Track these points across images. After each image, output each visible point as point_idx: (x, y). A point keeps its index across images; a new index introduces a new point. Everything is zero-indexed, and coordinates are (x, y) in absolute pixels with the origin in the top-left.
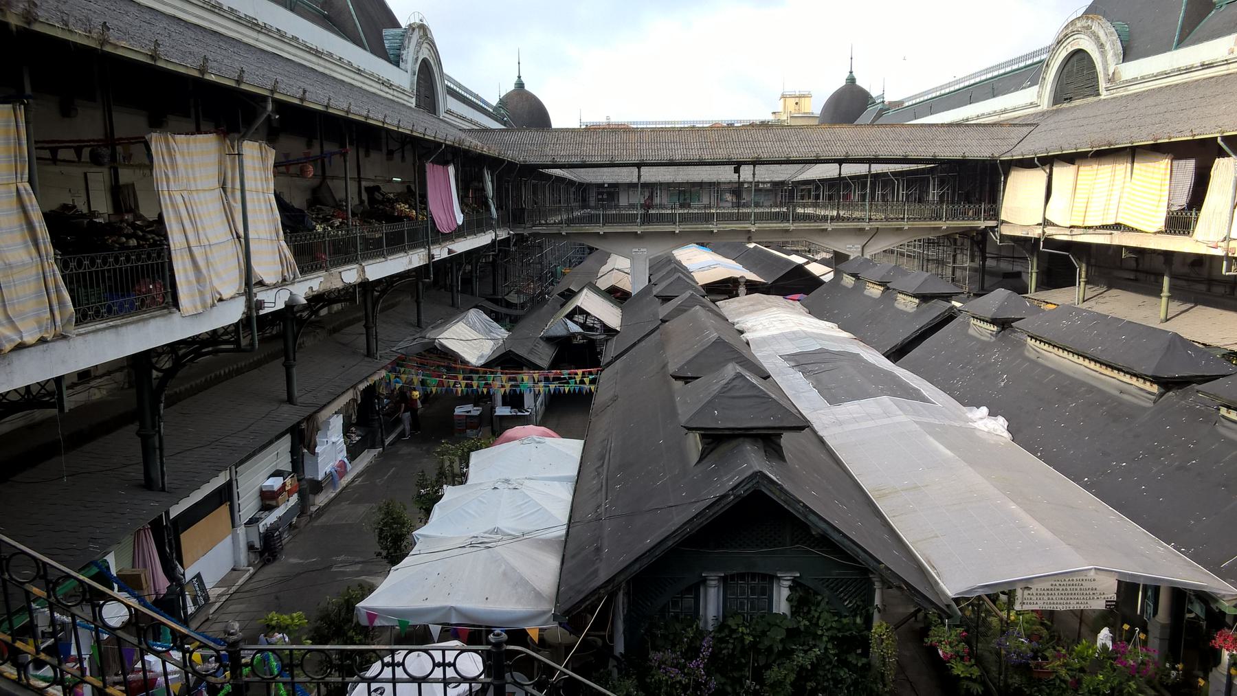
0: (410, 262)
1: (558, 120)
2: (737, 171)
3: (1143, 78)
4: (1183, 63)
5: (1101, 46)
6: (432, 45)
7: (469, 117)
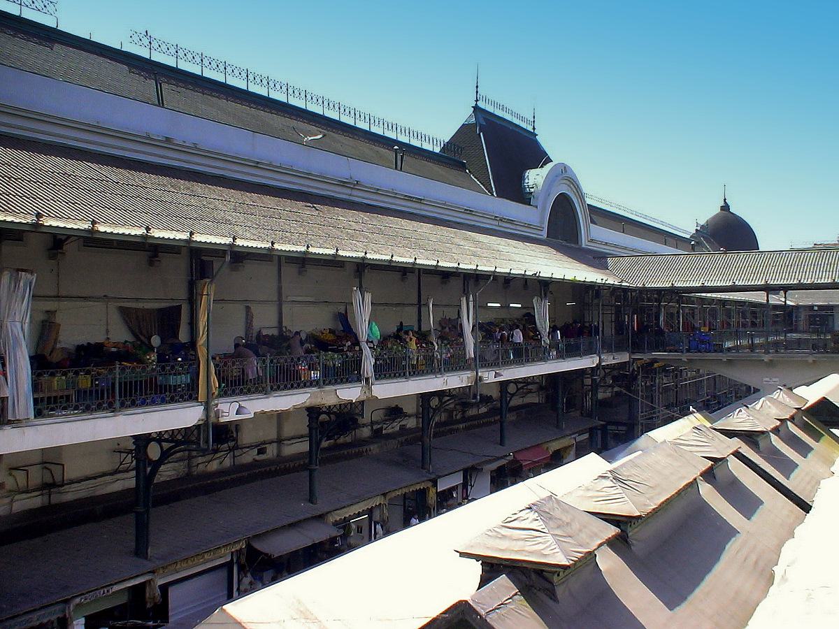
6: (573, 182)
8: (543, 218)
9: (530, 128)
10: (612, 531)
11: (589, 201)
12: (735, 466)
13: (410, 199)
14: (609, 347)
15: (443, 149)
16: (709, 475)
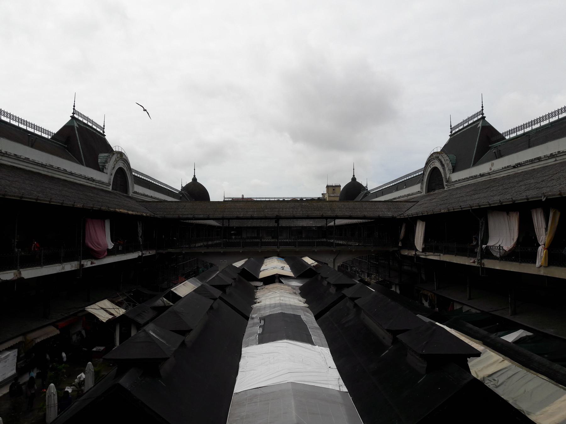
0: (63, 268)
2: (276, 222)
3: (459, 180)
4: (473, 174)
6: (126, 162)
7: (149, 194)
8: (110, 179)
9: (101, 132)
10: (180, 338)
11: (133, 173)
13: (38, 164)
14: (146, 248)
15: (52, 138)
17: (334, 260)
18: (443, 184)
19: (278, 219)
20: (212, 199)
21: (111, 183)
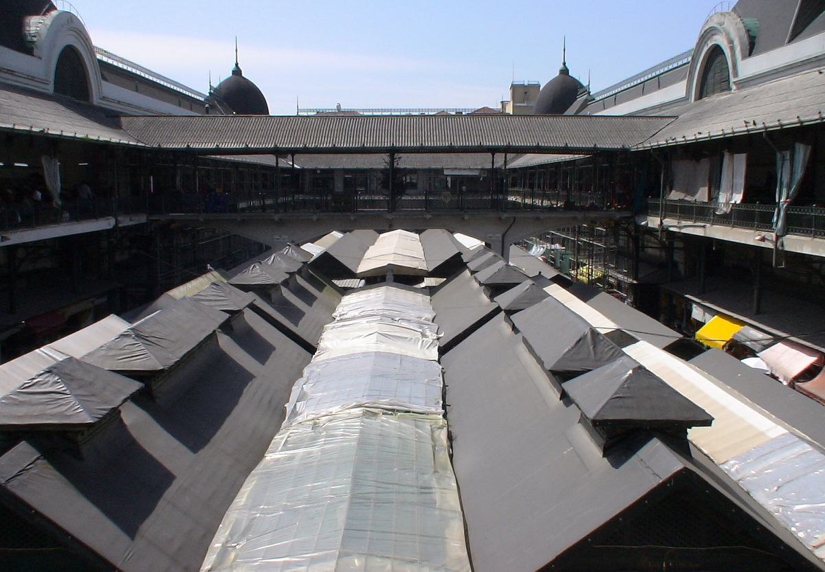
1: (276, 107)
5: (731, 42)
11: (99, 56)
12: (251, 318)
16: (226, 327)
17: (503, 236)
18: (728, 80)
19: (393, 151)
20: (273, 111)
21: (52, 78)
